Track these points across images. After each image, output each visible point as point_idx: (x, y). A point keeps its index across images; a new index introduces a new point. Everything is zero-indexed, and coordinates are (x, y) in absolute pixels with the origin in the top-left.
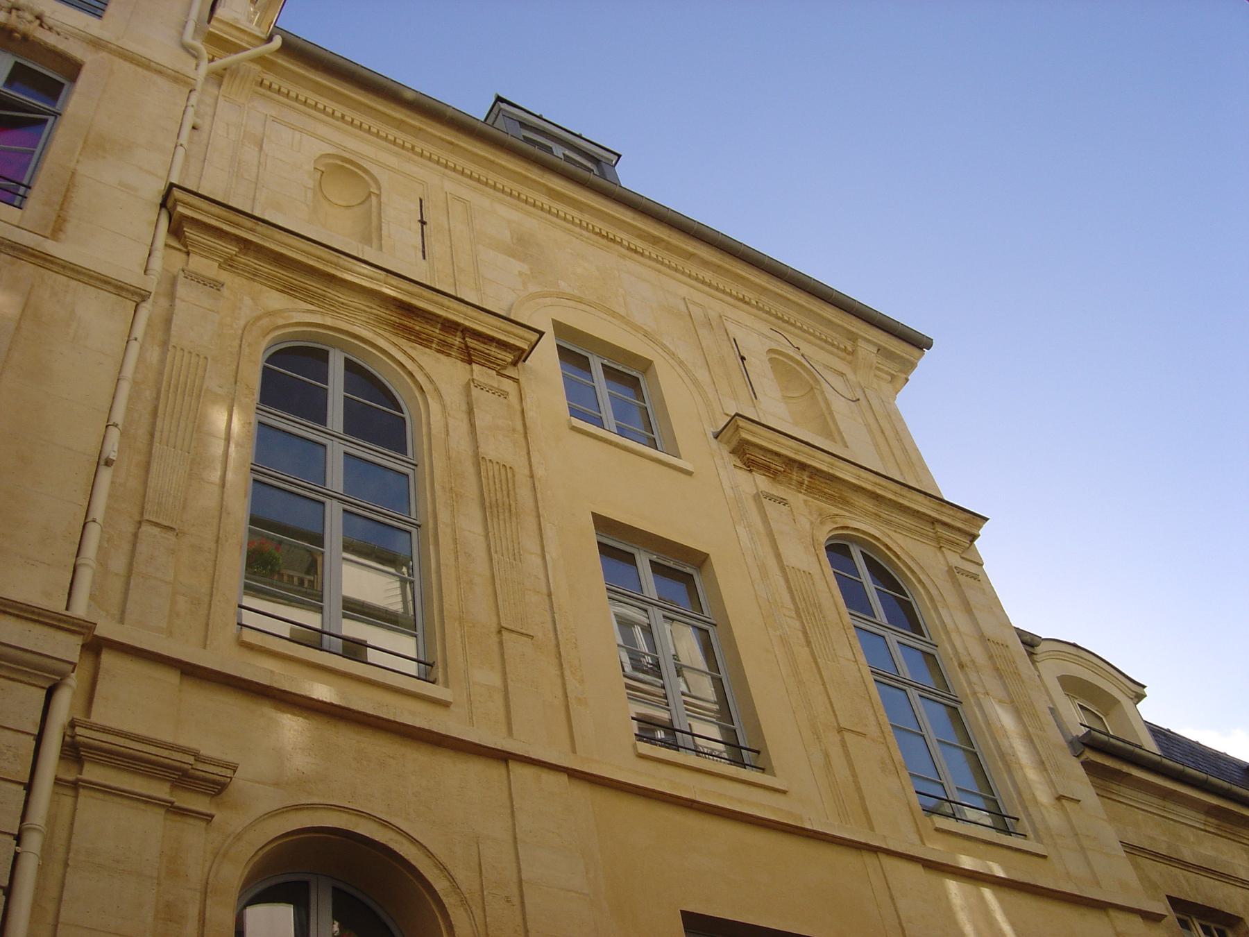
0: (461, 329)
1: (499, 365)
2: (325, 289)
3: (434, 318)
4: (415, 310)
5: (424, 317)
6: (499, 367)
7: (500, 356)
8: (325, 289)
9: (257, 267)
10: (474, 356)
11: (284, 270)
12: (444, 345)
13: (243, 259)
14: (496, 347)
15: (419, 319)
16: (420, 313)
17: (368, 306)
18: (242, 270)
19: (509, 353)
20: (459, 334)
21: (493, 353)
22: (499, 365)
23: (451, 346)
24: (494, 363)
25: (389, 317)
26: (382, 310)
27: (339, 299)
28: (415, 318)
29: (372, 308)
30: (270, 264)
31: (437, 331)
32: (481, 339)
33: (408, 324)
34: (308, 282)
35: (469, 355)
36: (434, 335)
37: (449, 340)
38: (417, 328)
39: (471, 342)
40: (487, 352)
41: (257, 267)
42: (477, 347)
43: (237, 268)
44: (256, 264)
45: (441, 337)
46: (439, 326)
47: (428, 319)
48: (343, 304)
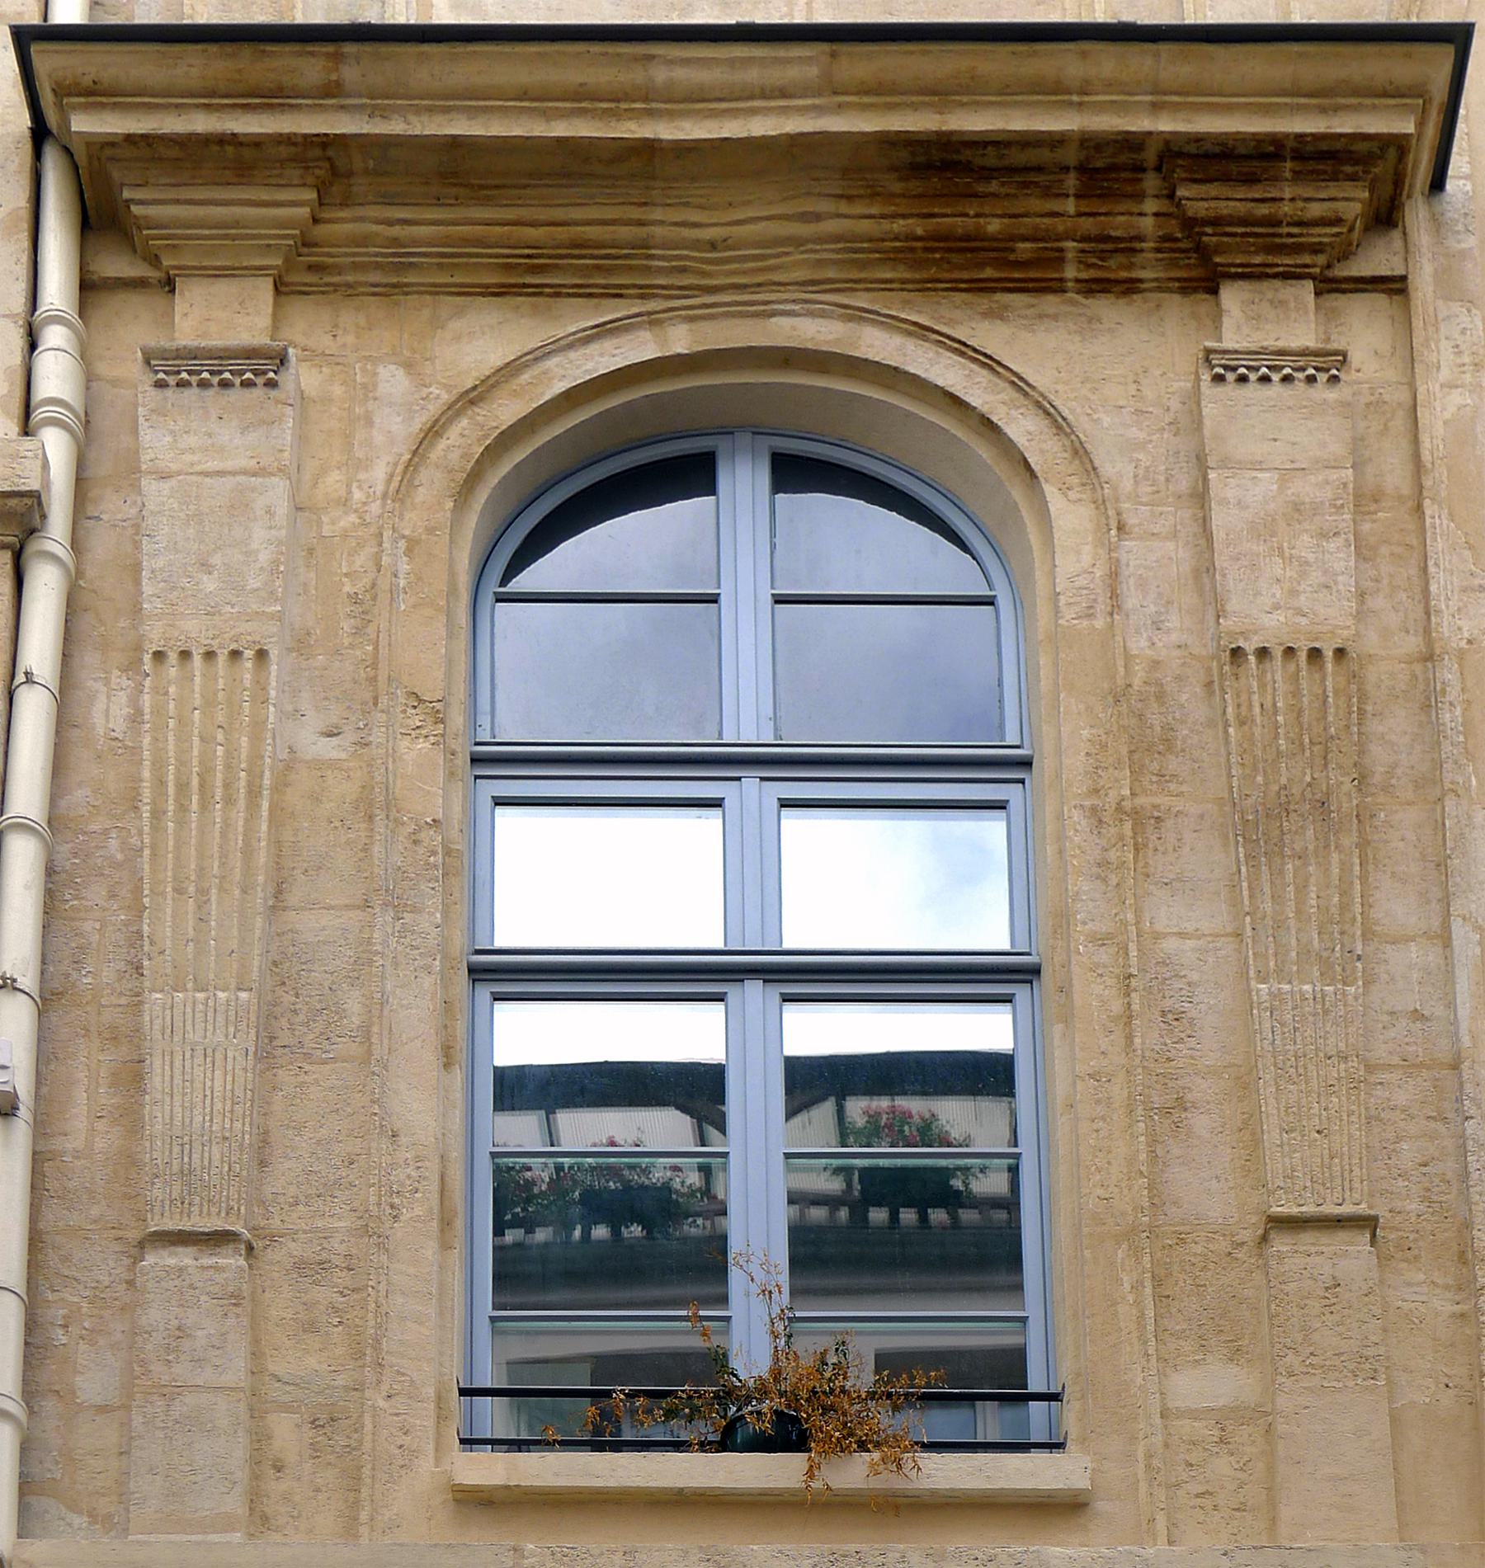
0: (1150, 156)
1: (1316, 249)
2: (635, 213)
3: (1044, 155)
4: (966, 155)
5: (1012, 170)
6: (1321, 259)
7: (1316, 210)
8: (635, 213)
9: (396, 231)
10: (1218, 250)
11: (486, 202)
12: (1103, 255)
13: (342, 225)
14: (1297, 176)
15: (994, 186)
16: (991, 159)
17: (804, 217)
18: (356, 267)
19: (1353, 178)
20: (1151, 182)
21: (1286, 208)
22: (1316, 249)
23: (1128, 246)
24: (1298, 249)
25: (886, 225)
26: (859, 209)
27: (688, 233)
28: (981, 188)
29: (817, 217)
30: (438, 202)
31: (1070, 206)
32: (1234, 168)
33: (960, 224)
34: (577, 214)
35: (1203, 253)
36: (1060, 225)
37: (1119, 225)
38: (994, 226)
39: (1200, 199)
40: (1263, 210)
41: (396, 231)
42: (1226, 208)
43: (339, 269)
44: (390, 223)
45: (1087, 225)
46: (1071, 182)
47: (1027, 169)
48: (713, 246)
